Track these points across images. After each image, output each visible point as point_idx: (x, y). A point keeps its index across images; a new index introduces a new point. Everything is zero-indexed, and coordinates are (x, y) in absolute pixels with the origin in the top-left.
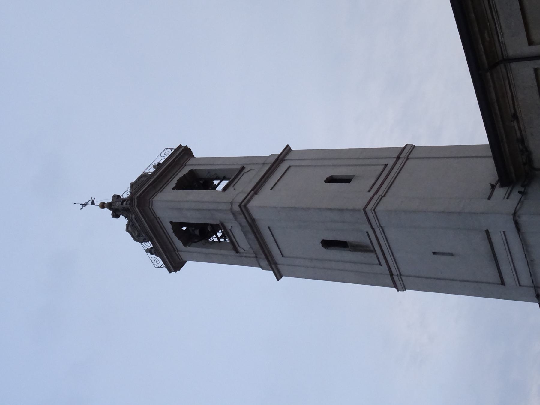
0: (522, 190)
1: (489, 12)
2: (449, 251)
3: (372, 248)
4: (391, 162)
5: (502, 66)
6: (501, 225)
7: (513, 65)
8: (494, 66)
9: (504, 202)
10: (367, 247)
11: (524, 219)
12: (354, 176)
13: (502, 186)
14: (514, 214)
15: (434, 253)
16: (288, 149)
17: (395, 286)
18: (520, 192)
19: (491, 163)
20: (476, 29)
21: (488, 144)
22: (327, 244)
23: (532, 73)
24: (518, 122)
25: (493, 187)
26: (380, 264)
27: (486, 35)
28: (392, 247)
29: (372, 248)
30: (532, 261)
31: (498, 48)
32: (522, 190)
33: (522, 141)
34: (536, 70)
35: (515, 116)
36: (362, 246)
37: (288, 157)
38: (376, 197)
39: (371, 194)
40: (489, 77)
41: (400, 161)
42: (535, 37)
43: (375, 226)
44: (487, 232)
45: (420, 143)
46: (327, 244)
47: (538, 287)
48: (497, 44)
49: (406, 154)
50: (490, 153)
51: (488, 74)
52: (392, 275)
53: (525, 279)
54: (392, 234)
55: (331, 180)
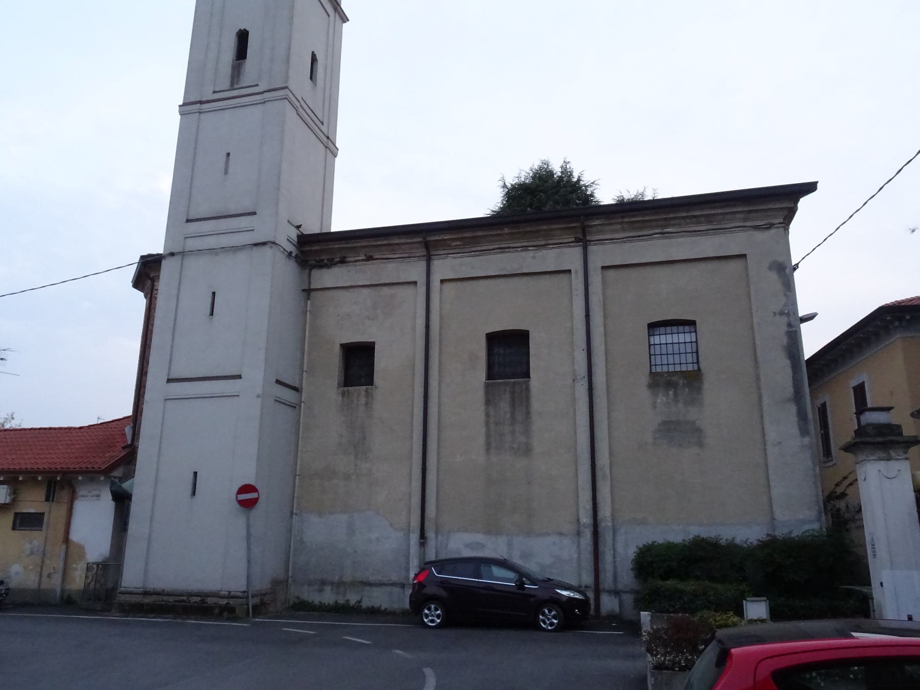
0: (293, 255)
1: (479, 248)
2: (230, 170)
3: (236, 86)
4: (324, 128)
5: (425, 253)
6: (262, 229)
7: (423, 264)
8: (427, 246)
9: (286, 236)
10: (237, 83)
11: (268, 251)
12: (316, 85)
13: (298, 236)
14: (274, 243)
15: (228, 154)
16: (345, 19)
17: (184, 104)
18: (291, 253)
19: (317, 231)
20: (466, 235)
21: (333, 230)
22: (243, 37)
23: (414, 280)
24: (363, 260)
25: (298, 227)
26: (214, 92)
27: (458, 243)
28: (237, 110)
29: (236, 86)
30: (217, 254)
31: (442, 252)
32: (293, 255)
33: (343, 261)
34: (415, 283)
35: (370, 258)
36: (238, 76)
37: (338, 17)
38: (298, 105)
39: (300, 99)
40: (415, 240)
41: (325, 139)
42: (448, 287)
43: (266, 95)
44: (255, 213)
45: (340, 162)
46: (243, 37)
47: (183, 255)
48: (445, 252)
49: (330, 147)
50: (324, 231)
51: (420, 240)
52: (201, 102)
53: (192, 244)
54: (257, 111)
55: (314, 59)
